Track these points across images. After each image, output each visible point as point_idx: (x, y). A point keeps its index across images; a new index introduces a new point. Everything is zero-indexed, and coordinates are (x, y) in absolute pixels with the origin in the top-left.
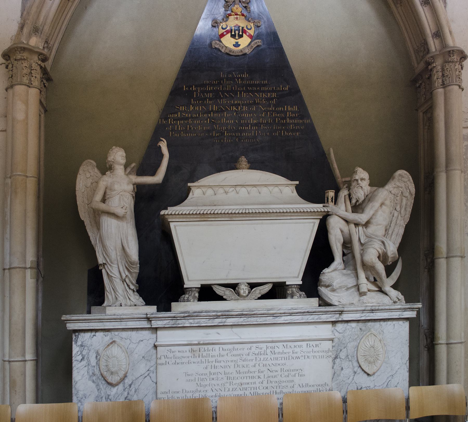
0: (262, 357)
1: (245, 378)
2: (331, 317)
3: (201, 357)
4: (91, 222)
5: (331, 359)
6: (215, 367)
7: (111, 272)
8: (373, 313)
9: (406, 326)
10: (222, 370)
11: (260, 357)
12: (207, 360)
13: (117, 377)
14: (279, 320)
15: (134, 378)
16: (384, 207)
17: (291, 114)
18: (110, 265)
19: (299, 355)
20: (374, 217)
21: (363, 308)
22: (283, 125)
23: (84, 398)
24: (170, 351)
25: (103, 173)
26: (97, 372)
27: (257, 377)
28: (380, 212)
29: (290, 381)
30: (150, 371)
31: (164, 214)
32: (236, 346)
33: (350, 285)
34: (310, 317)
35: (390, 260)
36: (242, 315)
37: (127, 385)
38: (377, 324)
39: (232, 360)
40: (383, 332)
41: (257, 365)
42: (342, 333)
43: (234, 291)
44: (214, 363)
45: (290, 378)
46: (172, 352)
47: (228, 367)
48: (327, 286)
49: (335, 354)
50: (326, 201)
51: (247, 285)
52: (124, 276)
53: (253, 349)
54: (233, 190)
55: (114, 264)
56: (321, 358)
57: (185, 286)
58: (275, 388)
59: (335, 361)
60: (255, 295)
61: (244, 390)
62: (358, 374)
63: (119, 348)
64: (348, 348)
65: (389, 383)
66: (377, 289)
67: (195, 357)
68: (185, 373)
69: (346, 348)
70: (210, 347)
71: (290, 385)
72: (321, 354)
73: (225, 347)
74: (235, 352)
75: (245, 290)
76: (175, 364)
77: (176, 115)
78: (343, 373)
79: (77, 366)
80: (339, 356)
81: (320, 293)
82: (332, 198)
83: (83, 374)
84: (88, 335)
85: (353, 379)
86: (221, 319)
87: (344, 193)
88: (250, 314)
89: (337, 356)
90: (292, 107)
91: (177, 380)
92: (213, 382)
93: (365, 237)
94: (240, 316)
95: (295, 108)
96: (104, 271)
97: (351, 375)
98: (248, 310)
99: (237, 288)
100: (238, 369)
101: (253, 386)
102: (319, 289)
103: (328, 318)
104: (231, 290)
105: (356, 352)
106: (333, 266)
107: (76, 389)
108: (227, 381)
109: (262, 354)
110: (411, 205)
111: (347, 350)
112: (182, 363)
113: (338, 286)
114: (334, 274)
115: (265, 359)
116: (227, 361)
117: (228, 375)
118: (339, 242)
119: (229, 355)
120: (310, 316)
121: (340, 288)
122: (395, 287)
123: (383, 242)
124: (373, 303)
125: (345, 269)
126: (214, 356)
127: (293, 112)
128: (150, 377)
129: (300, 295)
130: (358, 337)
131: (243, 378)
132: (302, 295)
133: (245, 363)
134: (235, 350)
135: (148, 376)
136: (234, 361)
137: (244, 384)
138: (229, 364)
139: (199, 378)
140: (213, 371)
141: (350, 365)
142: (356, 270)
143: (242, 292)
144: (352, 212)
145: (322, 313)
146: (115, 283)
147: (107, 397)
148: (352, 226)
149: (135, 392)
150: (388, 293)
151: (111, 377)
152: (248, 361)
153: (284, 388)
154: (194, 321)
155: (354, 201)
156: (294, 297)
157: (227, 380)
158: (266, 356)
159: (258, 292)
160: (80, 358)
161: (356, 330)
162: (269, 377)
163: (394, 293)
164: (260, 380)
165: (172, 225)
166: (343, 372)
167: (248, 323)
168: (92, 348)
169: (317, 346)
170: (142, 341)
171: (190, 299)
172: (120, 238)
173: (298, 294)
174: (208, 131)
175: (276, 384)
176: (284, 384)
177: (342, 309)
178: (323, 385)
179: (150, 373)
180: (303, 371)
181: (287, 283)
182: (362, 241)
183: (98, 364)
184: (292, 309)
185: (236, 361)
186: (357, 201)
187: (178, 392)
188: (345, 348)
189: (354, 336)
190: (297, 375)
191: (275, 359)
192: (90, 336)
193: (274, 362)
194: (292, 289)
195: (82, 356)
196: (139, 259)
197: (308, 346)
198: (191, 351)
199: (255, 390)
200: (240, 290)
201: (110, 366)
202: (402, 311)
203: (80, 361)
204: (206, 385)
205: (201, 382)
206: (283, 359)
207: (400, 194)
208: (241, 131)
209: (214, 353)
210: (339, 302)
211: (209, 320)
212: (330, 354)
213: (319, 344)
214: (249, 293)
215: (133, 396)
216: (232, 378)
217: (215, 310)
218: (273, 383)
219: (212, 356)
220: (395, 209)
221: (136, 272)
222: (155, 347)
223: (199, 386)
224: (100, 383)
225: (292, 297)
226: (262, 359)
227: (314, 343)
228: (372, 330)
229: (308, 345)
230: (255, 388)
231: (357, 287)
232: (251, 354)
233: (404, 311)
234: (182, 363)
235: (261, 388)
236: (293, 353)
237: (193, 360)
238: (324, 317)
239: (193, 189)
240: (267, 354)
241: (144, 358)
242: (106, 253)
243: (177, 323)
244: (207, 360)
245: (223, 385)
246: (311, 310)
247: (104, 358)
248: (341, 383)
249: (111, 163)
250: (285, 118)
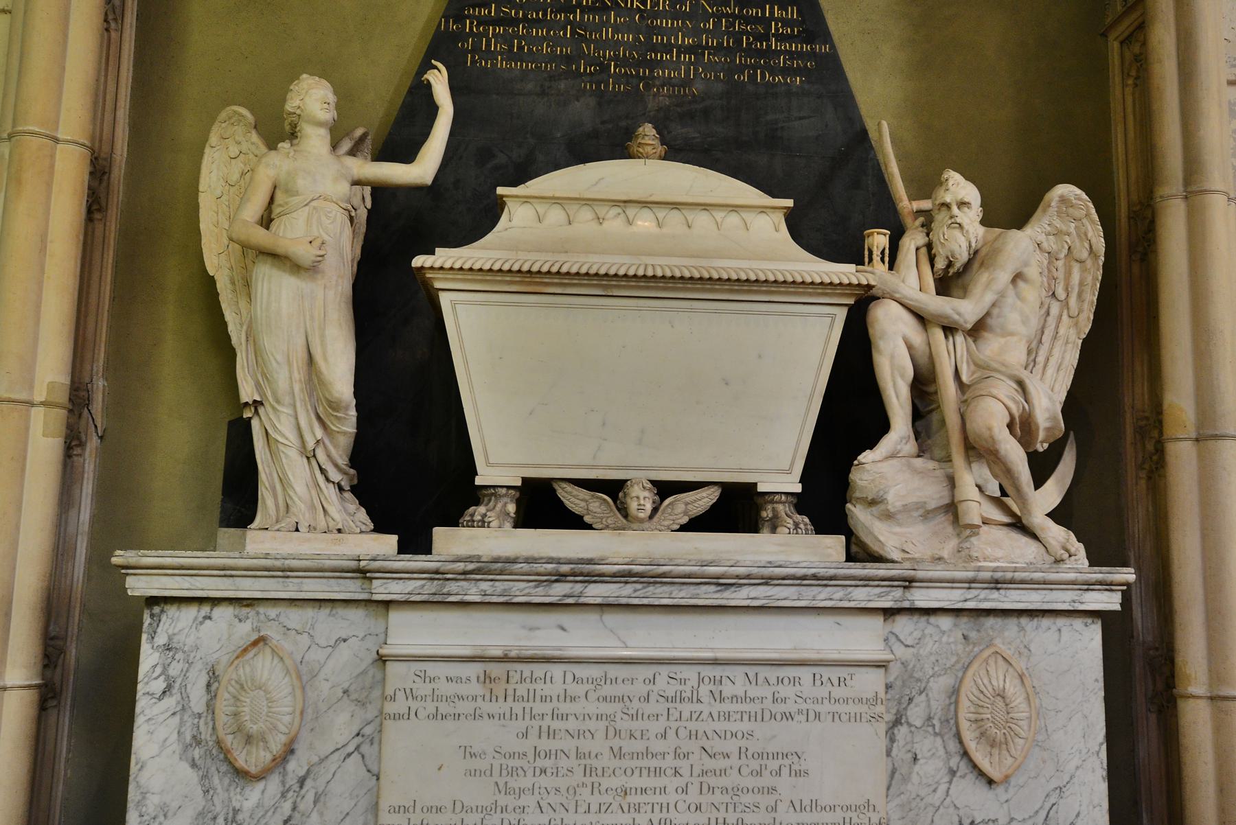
0: (686, 708)
1: (637, 772)
2: (879, 596)
3: (510, 699)
4: (233, 283)
5: (882, 727)
6: (552, 734)
7: (274, 427)
8: (998, 589)
9: (1093, 636)
10: (569, 744)
11: (679, 709)
12: (527, 711)
13: (262, 753)
14: (733, 596)
15: (315, 759)
16: (1021, 284)
17: (782, 27)
18: (274, 408)
19: (791, 707)
20: (995, 311)
21: (970, 575)
22: (761, 53)
23: (162, 818)
24: (422, 675)
25: (272, 146)
26: (206, 734)
27: (669, 772)
28: (1011, 298)
29: (766, 790)
30: (363, 736)
31: (422, 268)
32: (613, 671)
33: (932, 505)
34: (820, 592)
35: (1041, 435)
36: (630, 574)
37: (292, 781)
38: (1012, 623)
39: (599, 712)
40: (1030, 650)
41: (671, 734)
42: (912, 646)
43: (615, 502)
44: (548, 719)
45: (767, 780)
46: (427, 680)
47: (587, 734)
48: (873, 503)
49: (894, 711)
50: (866, 260)
51: (649, 485)
52: (311, 444)
53: (662, 681)
54: (619, 214)
55: (283, 405)
56: (853, 719)
57: (478, 481)
58: (723, 808)
59: (893, 733)
60: (671, 517)
61: (632, 810)
62: (961, 776)
63: (276, 660)
64: (930, 695)
65: (1051, 812)
66: (1006, 520)
67: (494, 698)
68: (463, 748)
69: (924, 694)
70: (539, 670)
71: (766, 800)
72: (852, 708)
73: (582, 671)
74: (608, 690)
75: (642, 502)
76: (435, 717)
77: (484, 12)
78: (918, 773)
79: (149, 713)
80: (907, 719)
81: (851, 522)
82: (883, 253)
83: (165, 740)
84: (190, 613)
85: (948, 792)
86: (570, 585)
87: (912, 242)
88: (651, 573)
89: (901, 716)
90: (783, 8)
91: (439, 769)
92: (544, 781)
93: (973, 367)
94: (622, 579)
95: (793, 13)
96: (255, 423)
97: (941, 779)
98: (647, 561)
99: (621, 494)
100: (616, 743)
101: (658, 798)
102: (849, 509)
103: (871, 598)
104: (605, 500)
105: (952, 708)
106: (887, 443)
107: (138, 786)
108: (584, 780)
109: (686, 700)
110: (1096, 285)
111: (928, 701)
112: (457, 716)
113: (899, 504)
114: (886, 467)
115: (695, 716)
116: (586, 716)
117: (588, 762)
118: (902, 376)
119: (592, 696)
120: (820, 589)
121: (906, 509)
122: (1057, 515)
123: (1021, 384)
124: (997, 560)
125: (919, 456)
126: (548, 699)
127: (786, 23)
128: (363, 757)
129: (796, 526)
130: (957, 662)
131: (629, 772)
132: (802, 526)
133: (636, 725)
134: (608, 681)
135: (356, 753)
136: (604, 717)
137: (633, 791)
138: (591, 725)
139: (504, 767)
140: (545, 744)
141: (937, 750)
142: (948, 459)
143: (633, 506)
144: (938, 294)
145: (853, 583)
146: (284, 460)
147: (231, 815)
148: (939, 334)
149: (315, 802)
150: (1038, 533)
151: (245, 751)
152: (645, 717)
153: (747, 810)
154: (492, 586)
155: (940, 264)
156: (779, 529)
157: (585, 775)
158: (698, 707)
159: (680, 508)
160: (160, 685)
161: (952, 640)
162: (704, 773)
163: (1057, 534)
164: (679, 782)
166: (917, 768)
167: (645, 601)
168: (198, 657)
169: (842, 684)
170: (345, 640)
171: (490, 519)
172: (302, 330)
173: (791, 521)
174: (568, 59)
175: (727, 798)
176: (747, 799)
177: (912, 573)
178: (862, 807)
179: (362, 743)
180: (802, 758)
181: (761, 488)
182: (965, 378)
183: (210, 707)
184: (771, 564)
185: (612, 716)
186: (950, 265)
187: (439, 810)
188: (921, 693)
189: (947, 659)
190: (785, 771)
191: (722, 718)
192: (196, 618)
193: (720, 726)
194: (775, 505)
195: (165, 680)
196: (356, 394)
197: (818, 683)
198: (482, 678)
199: (664, 815)
200: (629, 500)
201: (245, 715)
202: (1080, 590)
203: (157, 696)
204: (522, 791)
205: (509, 779)
206: (746, 717)
207: (1065, 251)
208: (653, 64)
209: (548, 689)
210: (904, 551)
211: (536, 587)
212: (880, 709)
213: (848, 678)
214: (655, 510)
215: (308, 817)
216: (600, 772)
217: (554, 555)
218: (717, 791)
219: (544, 699)
220: (1054, 293)
221: (345, 433)
223: (503, 792)
224: (213, 769)
225: (774, 530)
226: (686, 715)
227: (835, 673)
228: (998, 641)
229: (818, 677)
230: (665, 805)
231: (952, 509)
232: (653, 698)
233: (1087, 590)
234: (457, 716)
235: (681, 806)
236: (775, 700)
237: (487, 707)
238: (861, 596)
239: (510, 204)
240: (699, 700)
241: (348, 696)
242: (264, 375)
243: (445, 591)
244: (527, 711)
245: (571, 791)
246: (822, 572)
247: (231, 689)
248: (913, 805)
249: (295, 119)
250: (765, 37)
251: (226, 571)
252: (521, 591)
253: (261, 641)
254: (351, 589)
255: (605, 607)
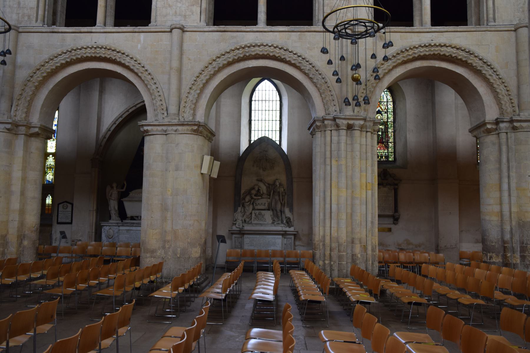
84: (105, 227)
165: (124, 202)
222: (119, 230)
251: (108, 223)
252: (129, 225)
253: (110, 229)
254: (117, 225)
255: (136, 226)
